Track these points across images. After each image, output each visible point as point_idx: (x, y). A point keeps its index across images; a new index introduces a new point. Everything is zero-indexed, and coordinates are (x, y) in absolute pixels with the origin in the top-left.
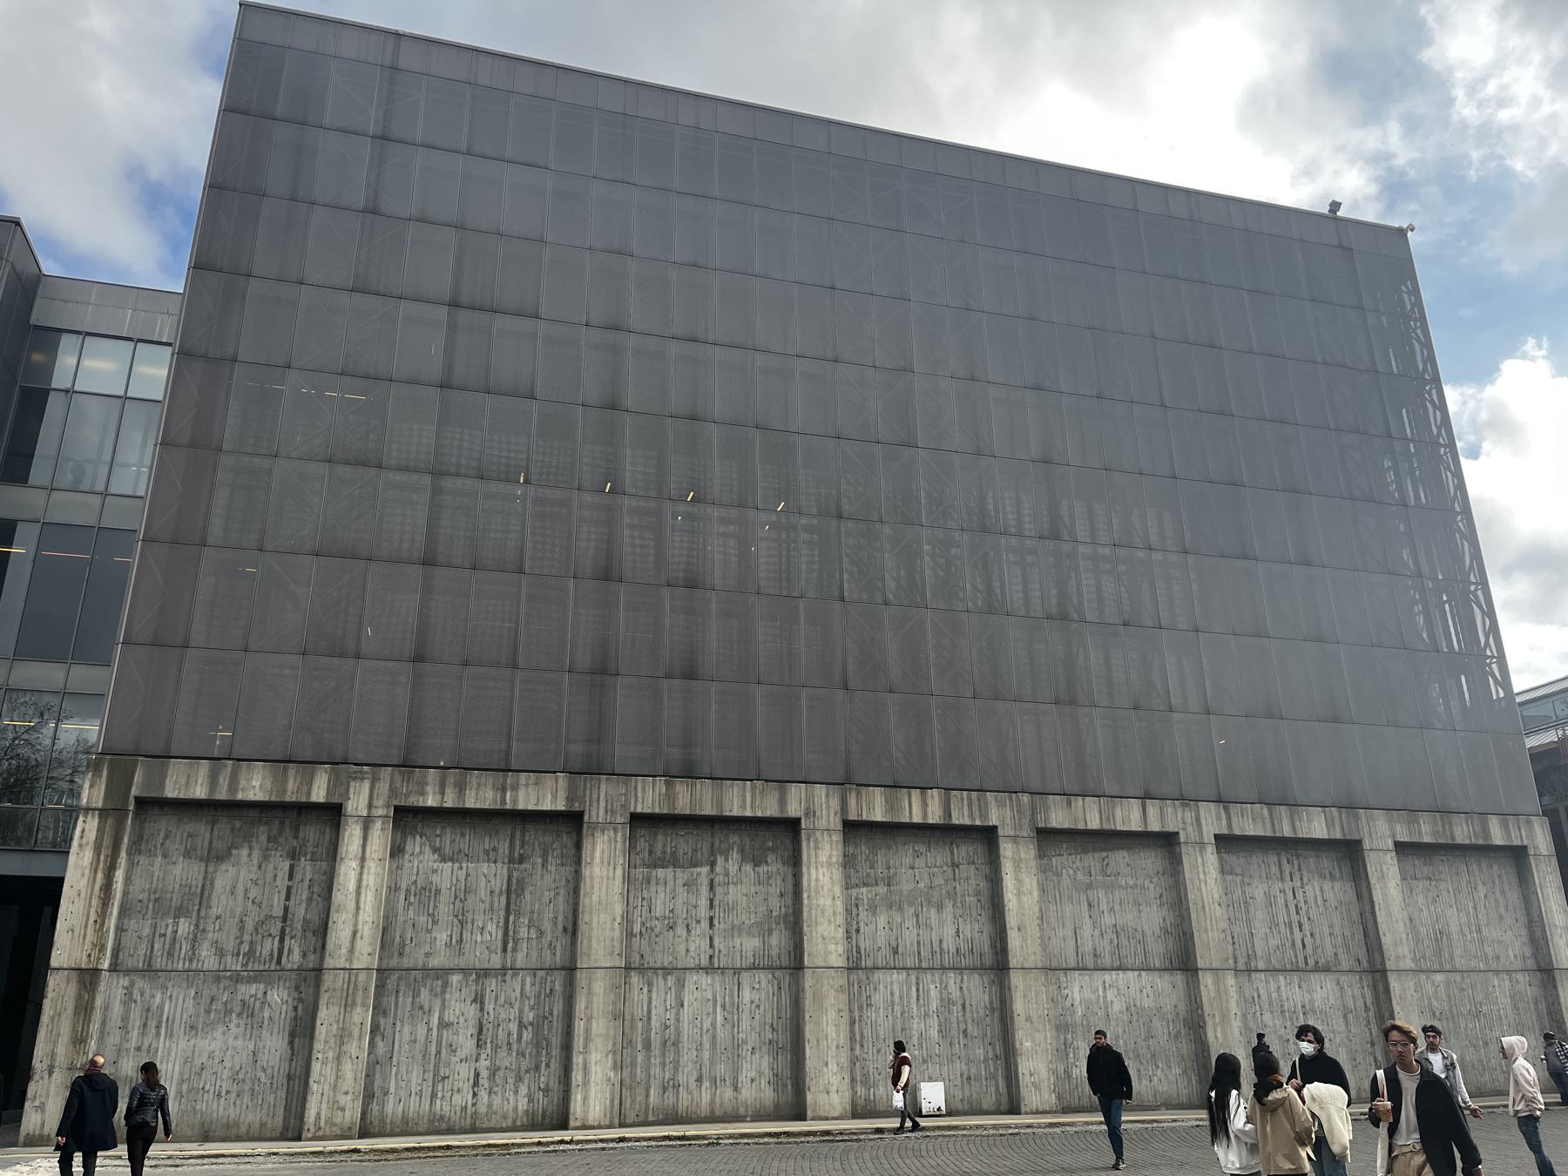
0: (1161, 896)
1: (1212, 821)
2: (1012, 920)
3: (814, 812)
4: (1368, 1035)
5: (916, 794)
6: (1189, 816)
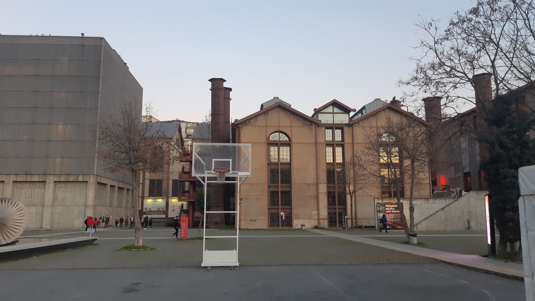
1: (13, 178)
6: (8, 177)
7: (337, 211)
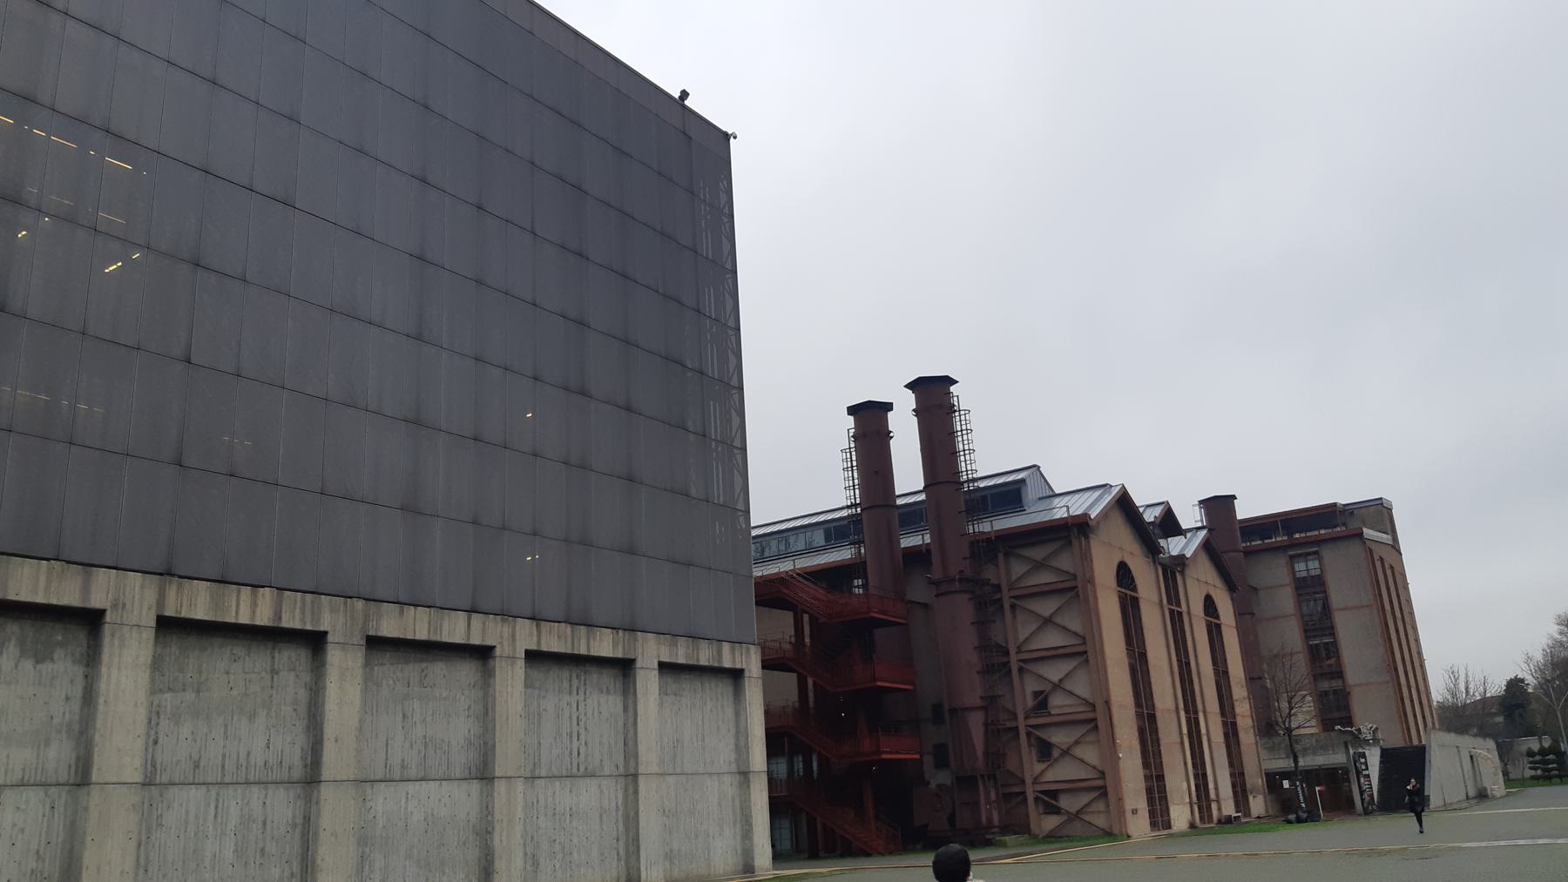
0: (469, 707)
2: (330, 731)
3: (124, 605)
4: (615, 832)
5: (246, 591)
6: (506, 630)
7: (1200, 772)
